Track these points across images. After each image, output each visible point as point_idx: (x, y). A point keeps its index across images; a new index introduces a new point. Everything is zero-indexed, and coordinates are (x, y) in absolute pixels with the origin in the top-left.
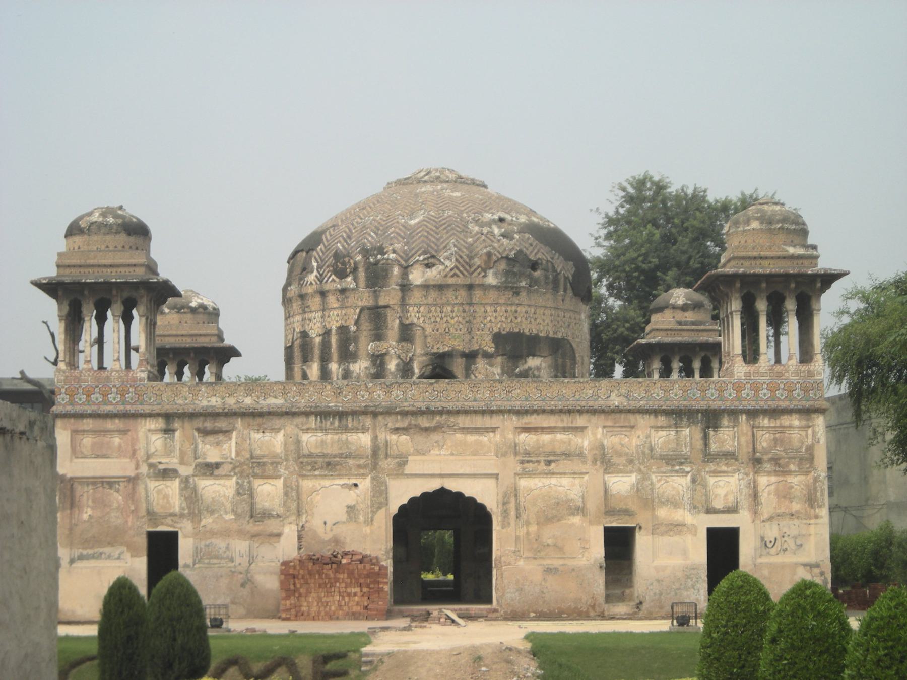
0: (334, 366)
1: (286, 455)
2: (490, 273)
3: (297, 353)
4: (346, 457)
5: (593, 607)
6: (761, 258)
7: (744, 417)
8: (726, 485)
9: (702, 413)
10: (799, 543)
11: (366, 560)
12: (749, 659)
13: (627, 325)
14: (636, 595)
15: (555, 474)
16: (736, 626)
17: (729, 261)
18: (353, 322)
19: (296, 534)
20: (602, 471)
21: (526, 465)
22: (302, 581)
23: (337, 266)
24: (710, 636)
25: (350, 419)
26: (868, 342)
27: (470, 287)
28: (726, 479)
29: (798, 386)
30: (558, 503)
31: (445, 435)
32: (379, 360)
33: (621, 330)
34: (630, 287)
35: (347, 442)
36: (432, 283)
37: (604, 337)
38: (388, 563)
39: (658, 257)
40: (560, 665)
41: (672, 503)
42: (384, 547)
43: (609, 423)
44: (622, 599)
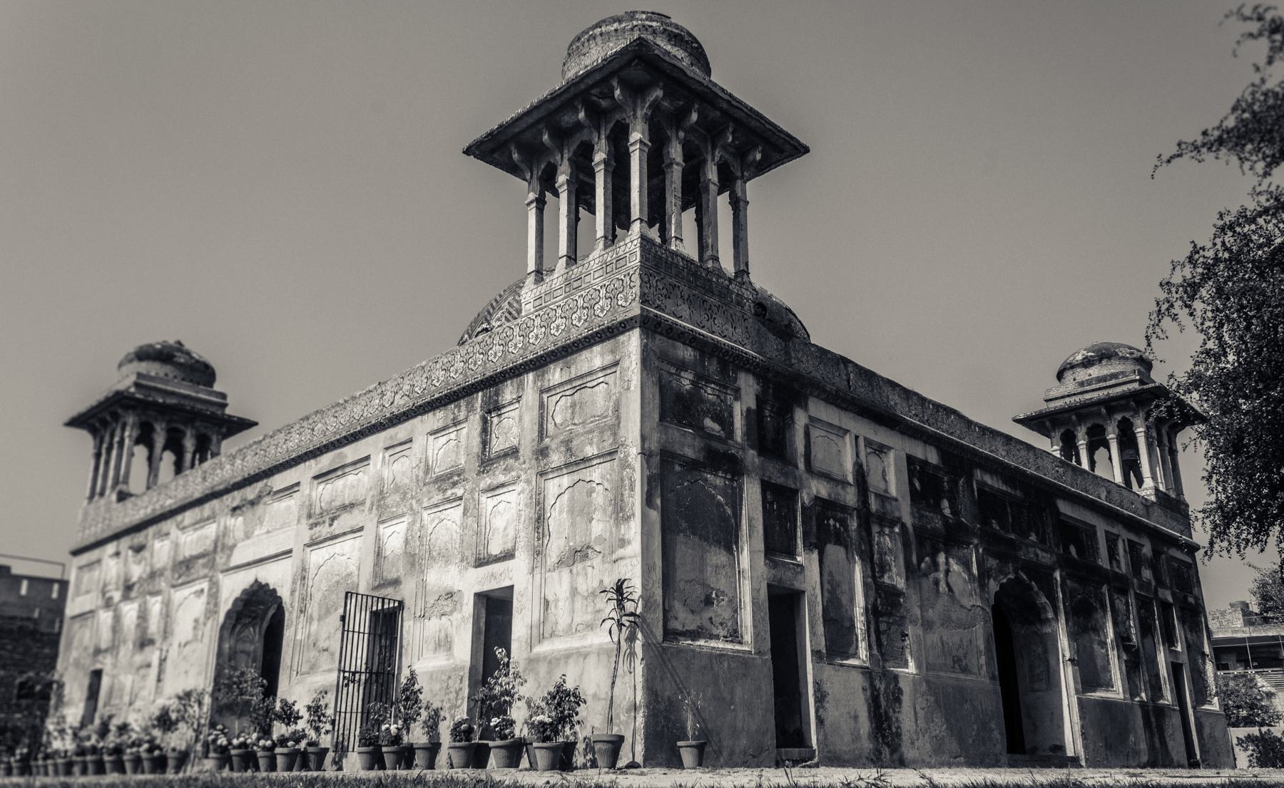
29: (603, 291)
30: (338, 582)
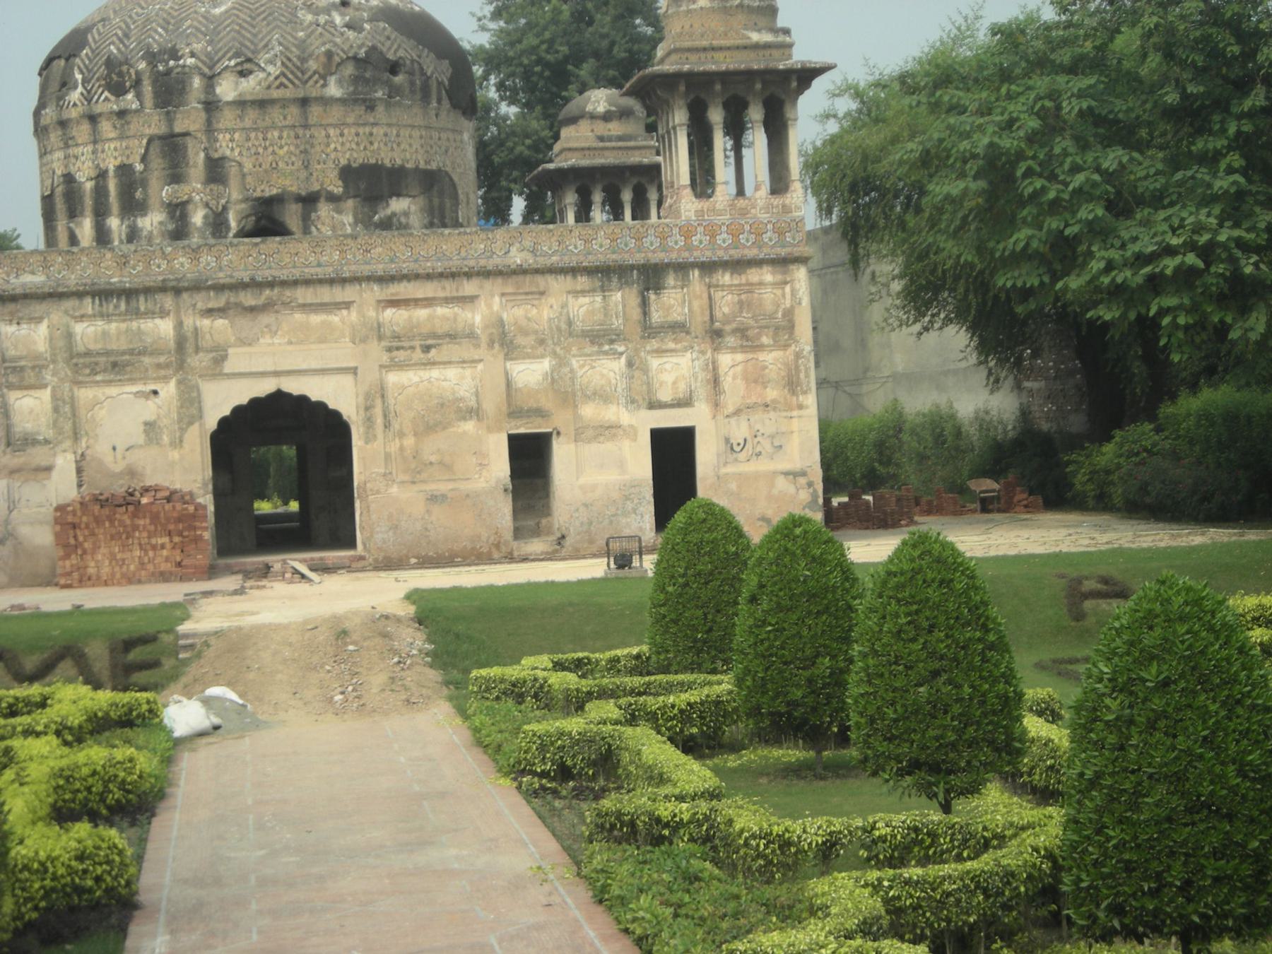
0: (114, 223)
1: (54, 355)
2: (332, 80)
3: (60, 205)
4: (140, 354)
5: (498, 546)
6: (713, 49)
7: (697, 272)
8: (675, 369)
9: (638, 270)
10: (776, 444)
11: (175, 497)
12: (718, 620)
13: (528, 142)
14: (557, 526)
15: (435, 363)
16: (699, 574)
17: (669, 54)
18: (138, 158)
19: (74, 466)
20: (501, 356)
21: (395, 353)
22: (86, 533)
23: (111, 79)
24: (663, 590)
25: (142, 299)
26: (865, 158)
27: (304, 102)
28: (674, 360)
29: (770, 227)
30: (442, 405)
31: (279, 316)
32: (178, 211)
33: (519, 149)
34: (531, 88)
35: (140, 332)
36: (249, 98)
37: (496, 160)
38: (207, 500)
39: (568, 43)
40: (457, 636)
41: (601, 396)
42: (199, 478)
43: (510, 289)
44: (536, 532)
